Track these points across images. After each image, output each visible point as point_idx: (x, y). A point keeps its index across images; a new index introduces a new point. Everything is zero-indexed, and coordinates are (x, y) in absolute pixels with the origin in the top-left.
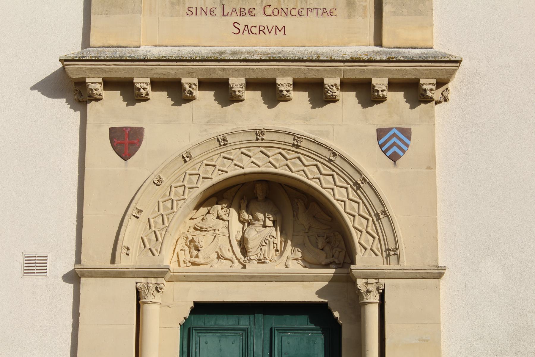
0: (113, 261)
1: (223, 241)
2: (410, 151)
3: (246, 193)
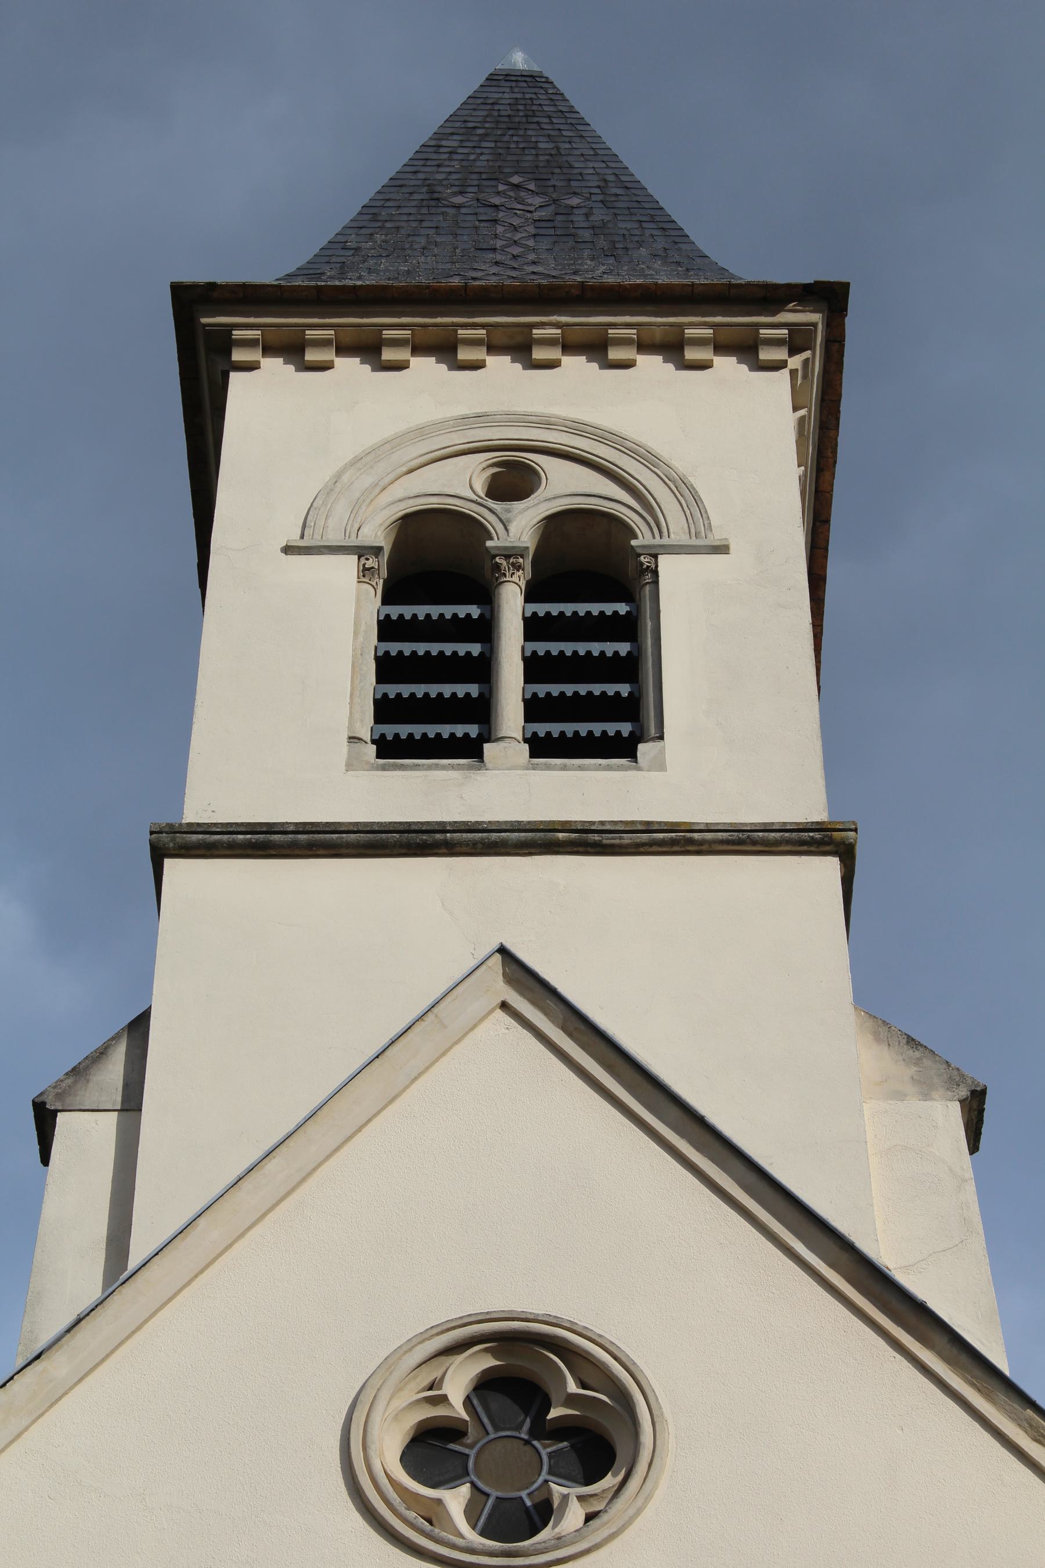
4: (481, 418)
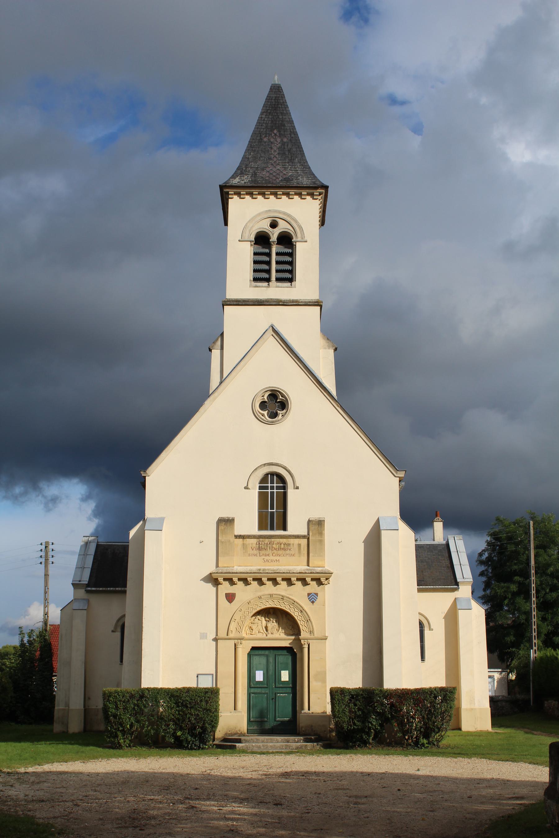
0: (227, 635)
1: (260, 627)
2: (317, 600)
3: (268, 613)
4: (270, 387)
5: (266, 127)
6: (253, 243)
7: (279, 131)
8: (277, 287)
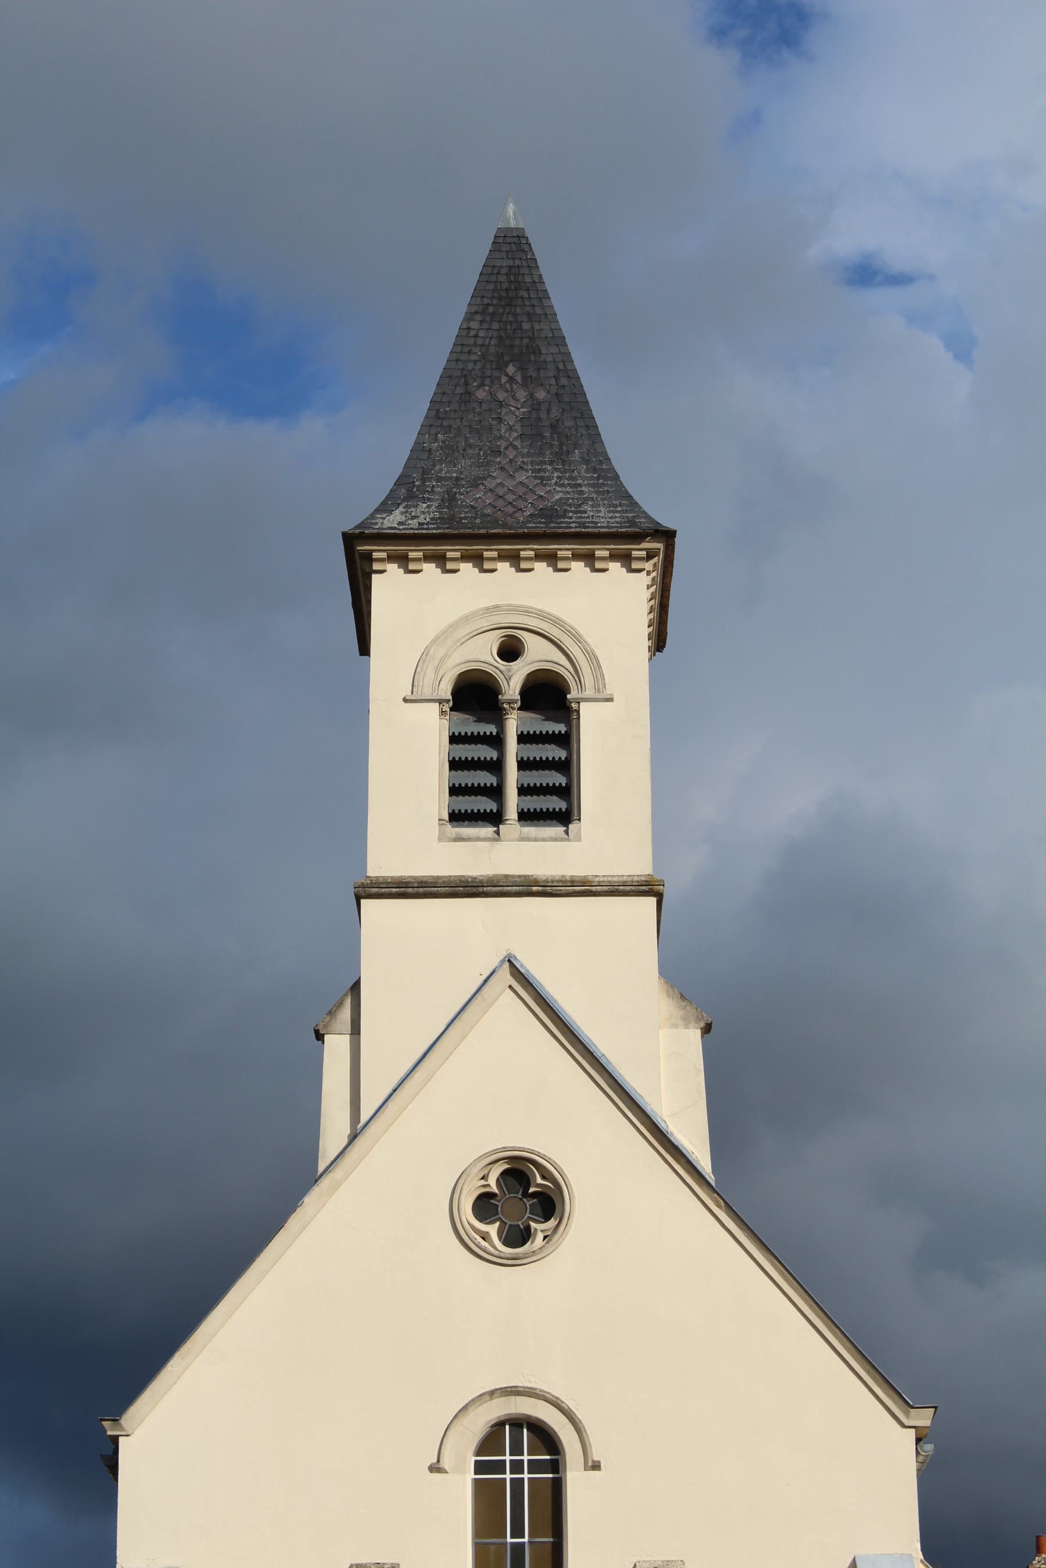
4: (505, 1149)
5: (483, 356)
6: (446, 708)
7: (522, 369)
8: (522, 839)
